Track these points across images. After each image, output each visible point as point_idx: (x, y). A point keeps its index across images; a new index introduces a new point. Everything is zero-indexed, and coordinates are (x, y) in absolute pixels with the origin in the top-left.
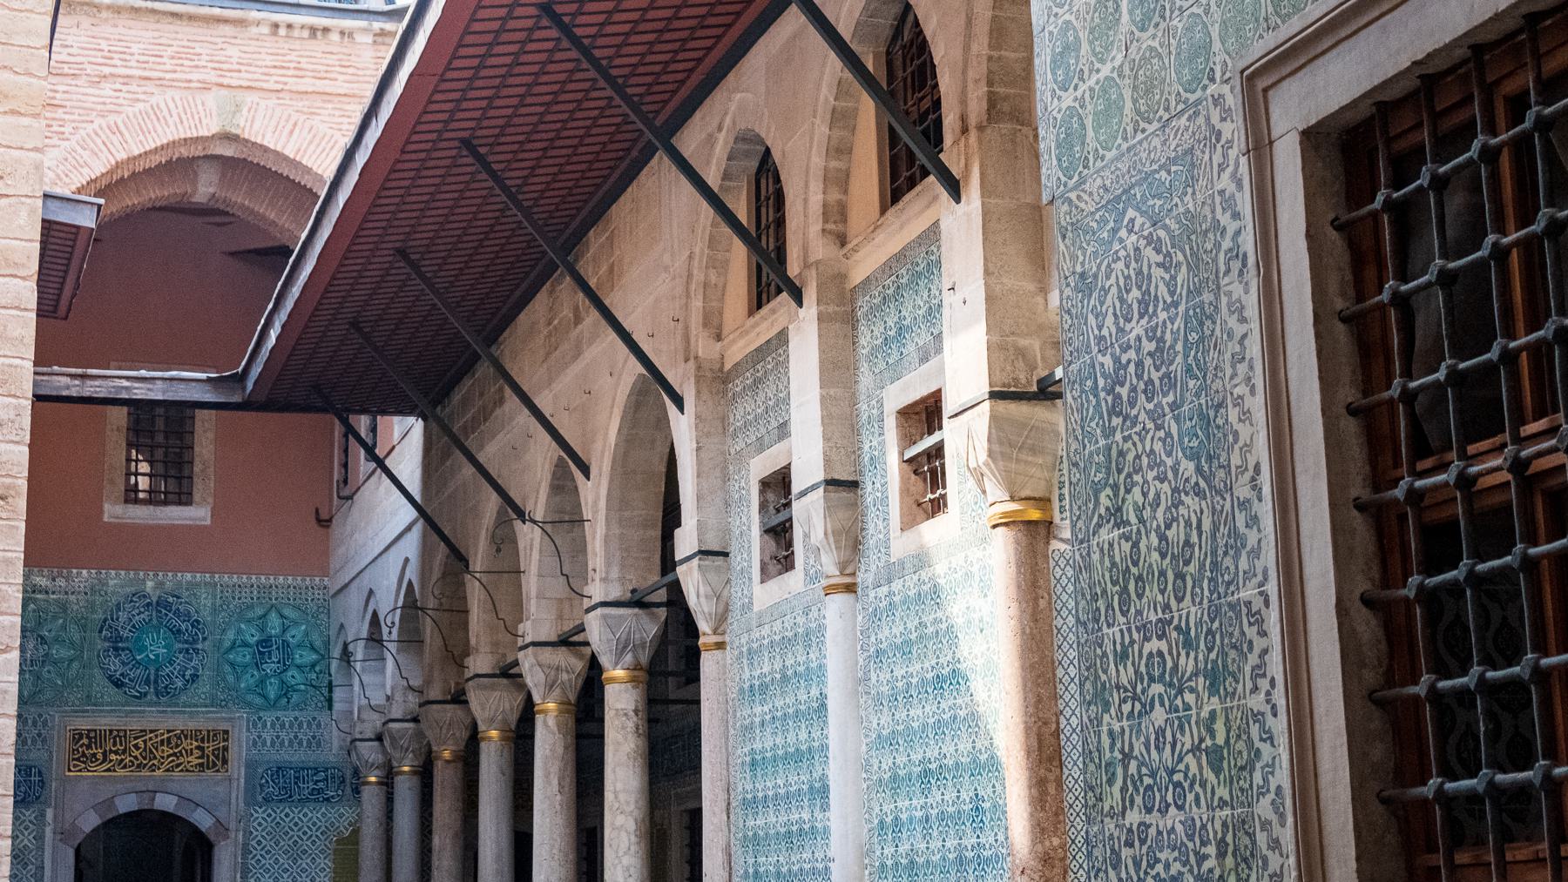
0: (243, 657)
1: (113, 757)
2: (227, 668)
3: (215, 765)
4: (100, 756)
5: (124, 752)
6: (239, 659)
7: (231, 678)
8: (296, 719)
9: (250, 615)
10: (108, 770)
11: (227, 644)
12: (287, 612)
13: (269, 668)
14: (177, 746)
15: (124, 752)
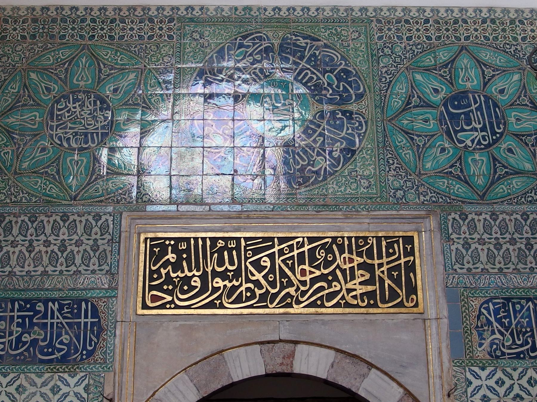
0: (424, 122)
1: (219, 283)
2: (401, 140)
3: (394, 295)
4: (197, 282)
5: (237, 274)
6: (419, 125)
7: (408, 155)
8: (525, 216)
9: (429, 61)
10: (211, 305)
11: (397, 103)
12: (486, 56)
13: (468, 137)
14: (328, 263)
15: (237, 274)
